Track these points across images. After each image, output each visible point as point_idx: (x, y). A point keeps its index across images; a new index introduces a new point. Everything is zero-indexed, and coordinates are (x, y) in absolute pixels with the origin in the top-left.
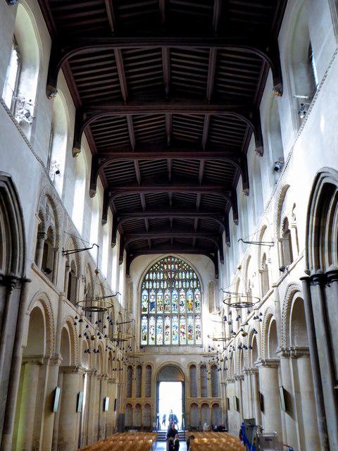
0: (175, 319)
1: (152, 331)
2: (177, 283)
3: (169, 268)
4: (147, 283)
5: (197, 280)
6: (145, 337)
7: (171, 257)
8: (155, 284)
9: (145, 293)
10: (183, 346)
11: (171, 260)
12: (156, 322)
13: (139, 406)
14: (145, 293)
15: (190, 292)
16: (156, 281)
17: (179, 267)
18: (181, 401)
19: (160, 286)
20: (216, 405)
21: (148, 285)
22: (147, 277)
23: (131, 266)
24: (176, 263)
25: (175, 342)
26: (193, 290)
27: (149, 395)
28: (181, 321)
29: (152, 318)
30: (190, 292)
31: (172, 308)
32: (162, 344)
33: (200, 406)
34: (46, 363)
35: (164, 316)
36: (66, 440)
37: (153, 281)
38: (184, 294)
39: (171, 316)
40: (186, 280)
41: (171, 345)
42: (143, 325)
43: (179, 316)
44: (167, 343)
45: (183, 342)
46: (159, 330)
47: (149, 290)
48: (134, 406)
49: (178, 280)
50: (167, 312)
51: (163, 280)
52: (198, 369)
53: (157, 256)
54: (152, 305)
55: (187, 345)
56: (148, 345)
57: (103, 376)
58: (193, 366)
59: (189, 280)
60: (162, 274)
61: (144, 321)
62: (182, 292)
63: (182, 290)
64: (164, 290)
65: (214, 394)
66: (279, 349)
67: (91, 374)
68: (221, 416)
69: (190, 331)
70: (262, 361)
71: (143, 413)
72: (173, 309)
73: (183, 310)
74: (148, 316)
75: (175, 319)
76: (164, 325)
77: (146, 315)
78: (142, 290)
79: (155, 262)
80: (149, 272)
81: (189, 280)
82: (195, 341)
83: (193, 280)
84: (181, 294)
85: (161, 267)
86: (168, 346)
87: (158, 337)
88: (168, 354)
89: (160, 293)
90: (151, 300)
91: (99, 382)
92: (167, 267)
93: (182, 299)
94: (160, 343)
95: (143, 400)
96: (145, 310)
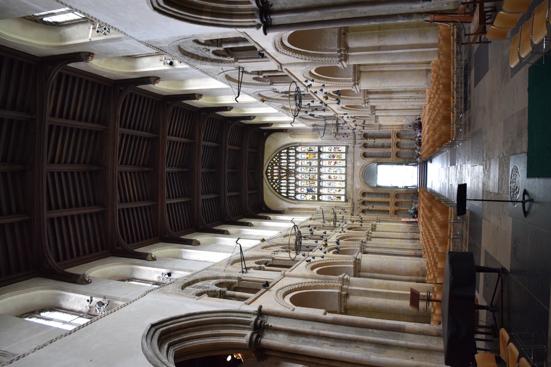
0: (322, 170)
1: (332, 192)
2: (290, 168)
3: (276, 174)
5: (288, 149)
6: (338, 197)
7: (267, 173)
8: (291, 188)
9: (298, 197)
10: (346, 163)
11: (269, 173)
12: (325, 187)
13: (396, 204)
14: (298, 197)
15: (299, 156)
16: (288, 186)
17: (276, 166)
19: (293, 183)
20: (398, 135)
22: (285, 195)
23: (274, 208)
24: (272, 168)
25: (343, 170)
26: (297, 153)
27: (387, 195)
28: (324, 165)
29: (322, 191)
30: (299, 156)
31: (313, 173)
32: (344, 182)
33: (398, 150)
35: (320, 180)
37: (288, 190)
38: (300, 161)
39: (320, 174)
40: (288, 159)
41: (346, 174)
42: (327, 200)
43: (320, 166)
44: (343, 177)
45: (343, 163)
46: (333, 184)
47: (296, 193)
49: (288, 166)
53: (265, 185)
54: (310, 191)
55: (346, 160)
56: (345, 195)
59: (288, 156)
60: (282, 181)
61: (323, 198)
62: (299, 163)
63: (297, 163)
64: (297, 180)
65: (389, 137)
69: (334, 157)
71: (403, 200)
72: (314, 172)
73: (315, 163)
74: (319, 194)
76: (328, 181)
78: (296, 199)
79: (271, 187)
80: (280, 193)
81: (288, 156)
82: (343, 153)
83: (288, 153)
84: (300, 164)
85: (276, 182)
86: (346, 177)
87: (338, 186)
88: (353, 177)
89: (299, 183)
90: (305, 191)
92: (276, 176)
93: (305, 163)
94: (343, 185)
96: (313, 198)
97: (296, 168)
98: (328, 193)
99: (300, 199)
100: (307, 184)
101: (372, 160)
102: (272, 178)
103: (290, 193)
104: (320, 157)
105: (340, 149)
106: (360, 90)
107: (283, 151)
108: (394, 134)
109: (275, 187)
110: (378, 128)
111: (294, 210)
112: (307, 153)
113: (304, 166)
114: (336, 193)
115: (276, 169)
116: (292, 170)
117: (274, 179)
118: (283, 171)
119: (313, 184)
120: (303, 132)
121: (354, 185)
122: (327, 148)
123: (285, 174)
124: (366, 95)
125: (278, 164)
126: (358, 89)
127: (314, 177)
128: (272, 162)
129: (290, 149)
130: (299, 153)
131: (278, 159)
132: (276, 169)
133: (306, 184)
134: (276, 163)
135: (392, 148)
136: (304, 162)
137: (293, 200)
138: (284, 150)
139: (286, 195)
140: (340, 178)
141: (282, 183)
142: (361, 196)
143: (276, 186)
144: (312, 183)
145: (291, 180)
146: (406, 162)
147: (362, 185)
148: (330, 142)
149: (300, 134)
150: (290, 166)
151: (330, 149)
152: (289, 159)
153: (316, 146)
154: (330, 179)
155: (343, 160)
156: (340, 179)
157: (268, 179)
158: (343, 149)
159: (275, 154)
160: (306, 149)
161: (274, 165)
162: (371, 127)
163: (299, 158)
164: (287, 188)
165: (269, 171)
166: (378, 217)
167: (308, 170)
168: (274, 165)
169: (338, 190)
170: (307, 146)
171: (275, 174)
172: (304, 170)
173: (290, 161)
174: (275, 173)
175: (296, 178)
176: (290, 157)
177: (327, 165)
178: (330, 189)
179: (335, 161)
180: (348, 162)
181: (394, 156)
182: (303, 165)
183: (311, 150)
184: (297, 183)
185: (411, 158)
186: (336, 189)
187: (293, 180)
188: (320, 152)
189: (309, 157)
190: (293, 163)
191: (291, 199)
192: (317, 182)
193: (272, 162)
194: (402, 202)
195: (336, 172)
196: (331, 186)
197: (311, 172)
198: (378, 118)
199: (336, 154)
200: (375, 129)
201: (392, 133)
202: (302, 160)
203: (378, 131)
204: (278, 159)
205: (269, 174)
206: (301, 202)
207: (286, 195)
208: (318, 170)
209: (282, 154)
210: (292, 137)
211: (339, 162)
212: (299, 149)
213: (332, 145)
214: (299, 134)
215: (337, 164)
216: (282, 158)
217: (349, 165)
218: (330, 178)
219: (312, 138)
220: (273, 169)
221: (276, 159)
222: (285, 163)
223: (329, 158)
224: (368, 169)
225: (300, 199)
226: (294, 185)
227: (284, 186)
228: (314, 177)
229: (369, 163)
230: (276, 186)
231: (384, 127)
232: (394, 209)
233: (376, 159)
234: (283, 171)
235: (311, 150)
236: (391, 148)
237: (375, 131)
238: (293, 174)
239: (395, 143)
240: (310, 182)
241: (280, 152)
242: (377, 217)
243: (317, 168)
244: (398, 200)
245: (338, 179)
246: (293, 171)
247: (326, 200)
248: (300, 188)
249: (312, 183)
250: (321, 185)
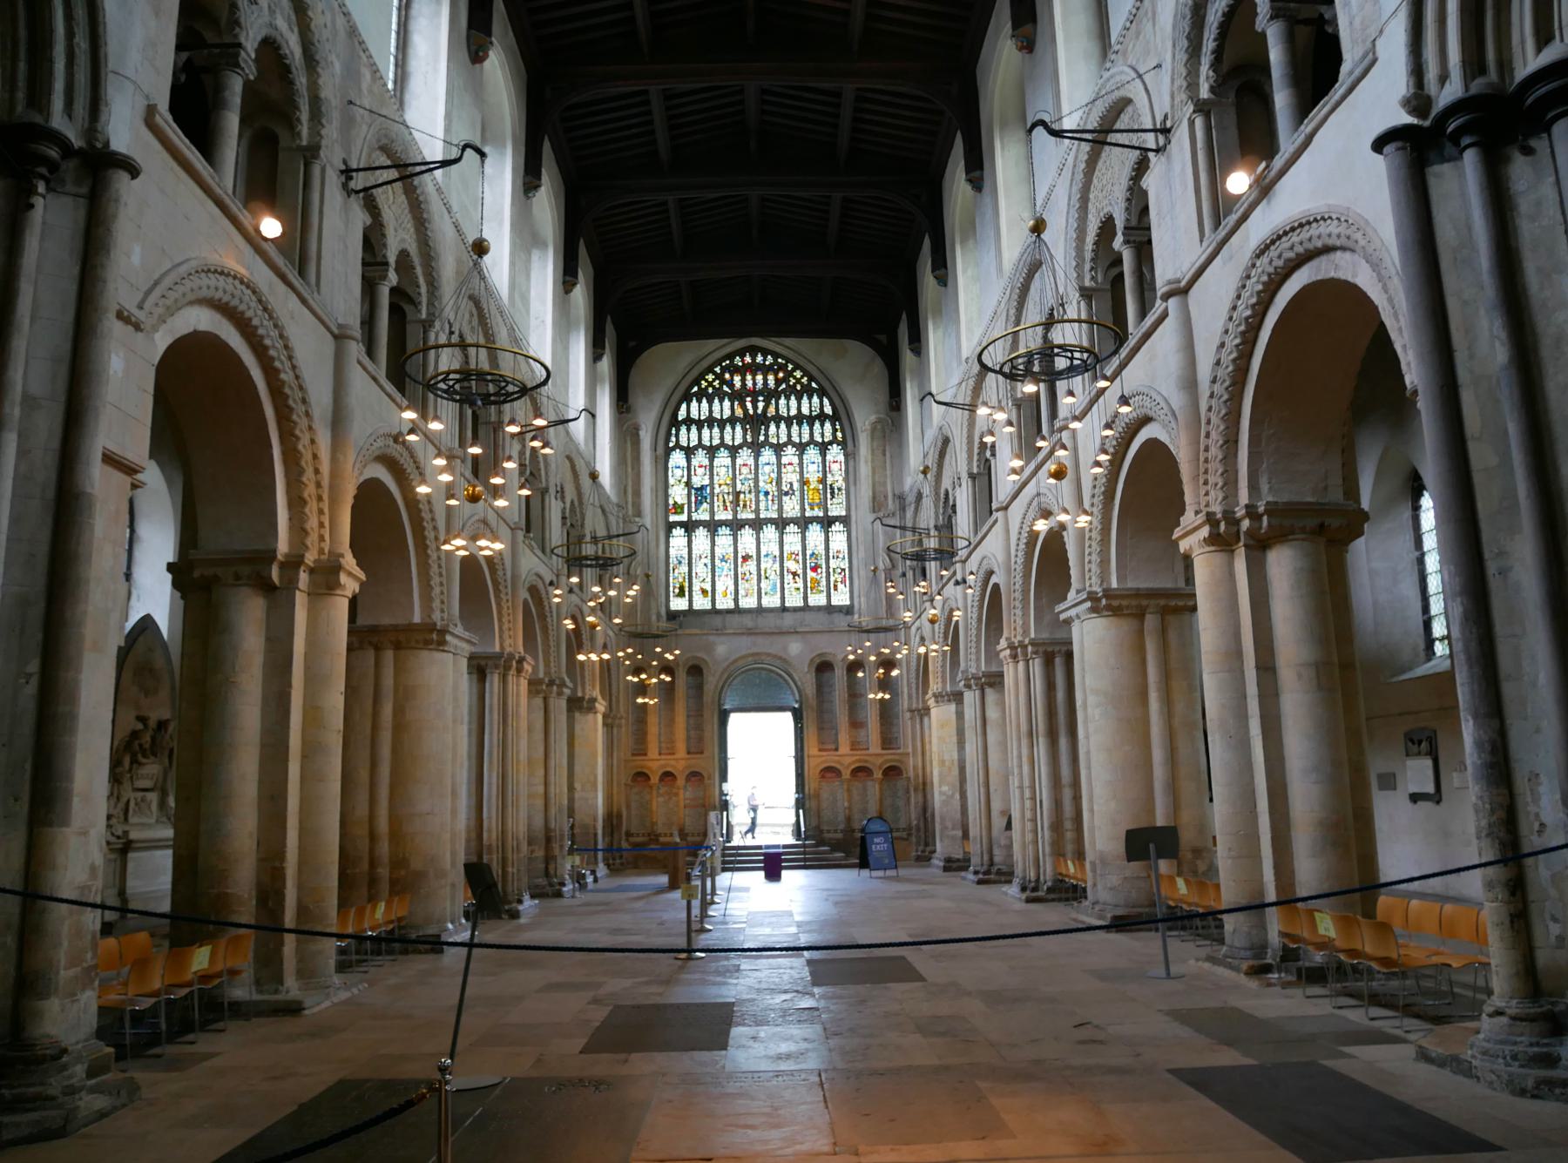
0: (770, 533)
1: (701, 570)
2: (773, 428)
3: (749, 384)
4: (683, 429)
5: (834, 418)
7: (753, 351)
8: (706, 432)
9: (677, 458)
10: (796, 610)
11: (754, 359)
13: (668, 776)
15: (812, 454)
16: (711, 421)
17: (778, 382)
18: (792, 762)
19: (722, 438)
20: (892, 772)
21: (688, 437)
22: (682, 414)
23: (635, 377)
25: (771, 601)
26: (823, 448)
30: (812, 454)
32: (731, 605)
33: (846, 774)
34: (291, 584)
35: (736, 526)
36: (416, 864)
37: (700, 424)
38: (795, 460)
39: (757, 525)
40: (800, 418)
41: (760, 610)
42: (672, 552)
43: (781, 524)
44: (748, 602)
45: (795, 600)
47: (689, 452)
48: (655, 779)
49: (778, 419)
50: (747, 515)
51: (733, 420)
52: (840, 674)
53: (712, 344)
54: (700, 495)
55: (806, 608)
56: (691, 612)
57: (551, 683)
58: (823, 667)
59: (811, 420)
60: (727, 403)
62: (790, 455)
63: (790, 450)
64: (734, 451)
65: (888, 741)
66: (1189, 518)
67: (507, 668)
68: (908, 800)
69: (814, 569)
70: (1092, 597)
71: (681, 796)
72: (762, 505)
73: (791, 507)
74: (689, 527)
75: (770, 533)
77: (681, 524)
78: (668, 452)
79: (705, 364)
80: (687, 398)
81: (811, 420)
83: (822, 417)
85: (723, 382)
86: (749, 611)
87: (720, 588)
88: (750, 632)
89: (723, 459)
90: (697, 481)
91: (539, 701)
92: (743, 380)
93: (790, 476)
94: (724, 603)
95: (679, 762)
96: (678, 508)
97: (772, 446)
98: (694, 556)
99: (670, 466)
100: (720, 485)
101: (810, 690)
102: (735, 370)
103: (689, 430)
104: (812, 523)
105: (840, 586)
106: (1068, 622)
107: (826, 401)
108: (897, 757)
109: (706, 381)
110: (914, 706)
111: (632, 444)
112: (823, 481)
113: (779, 473)
114: (694, 580)
115: (765, 380)
116: (767, 435)
117: (732, 376)
118: (761, 405)
119: (721, 504)
120: (892, 462)
121: (723, 638)
122: (843, 547)
123: (751, 412)
124: (1041, 649)
125: (784, 386)
126: (1072, 613)
127: (745, 506)
128: (790, 367)
129: (833, 425)
130: (823, 455)
131: (799, 387)
132: (765, 380)
133: (721, 482)
134: (785, 380)
135: (852, 755)
136: (795, 471)
137: (668, 440)
138: (832, 404)
139: (680, 418)
140: (747, 590)
141: (721, 401)
142: (690, 663)
143: (710, 384)
144: (724, 501)
145: (733, 432)
146: (807, 802)
147: (727, 663)
148: (861, 554)
149: (884, 455)
150: (778, 427)
151: (841, 556)
152: (800, 424)
153: (848, 509)
154: (740, 560)
155: (805, 598)
156: (742, 592)
157: (731, 356)
158: (841, 598)
159: (815, 373)
160: (836, 478)
161: (781, 375)
162: (917, 684)
163: (805, 457)
164: (705, 421)
165: (759, 359)
166: (623, 721)
167: (768, 487)
168: (781, 375)
169: (708, 587)
170: (846, 479)
171: (749, 377)
172: (767, 472)
173: (795, 428)
174: (754, 380)
175: (740, 446)
176: (808, 424)
177: (786, 548)
178: (708, 561)
179: (800, 572)
180: (799, 615)
181: (825, 762)
182: (784, 470)
183: (832, 494)
184: (723, 453)
185: (819, 817)
186: (709, 579)
187: (733, 439)
188: (827, 522)
189: (812, 487)
190: (789, 436)
191: (669, 434)
192: (730, 517)
193: (790, 367)
194: (677, 795)
195: (763, 577)
196: (717, 562)
197: (762, 497)
198: (949, 701)
199: (824, 575)
200: (910, 696)
201: (898, 751)
202: (801, 464)
203: (906, 706)
204: (799, 387)
205: (748, 359)
206: (661, 467)
207: (680, 418)
208: (771, 519)
209: (815, 399)
210: (873, 430)
211: (796, 586)
212: (835, 453)
213: (855, 562)
214: (884, 451)
215: (792, 581)
216: (805, 400)
217: (788, 620)
218: (746, 558)
219: (874, 493)
220: (765, 370)
221: (798, 381)
222: (788, 410)
223: (809, 552)
224: (781, 680)
225: (671, 464)
226: (716, 442)
227: (711, 411)
228: (745, 506)
229: (799, 683)
230: (710, 384)
231: (918, 726)
232: (649, 768)
233: (813, 702)
234: (761, 405)
235: (832, 494)
236: (852, 750)
237: (906, 696)
238: (752, 437)
239: (866, 761)
240: (728, 493)
241: (822, 393)
242: (621, 718)
243: (775, 515)
244: (681, 781)
245: (742, 586)
246: (762, 438)
247: (671, 549)
248: (706, 462)
249: (724, 501)
250: (720, 533)
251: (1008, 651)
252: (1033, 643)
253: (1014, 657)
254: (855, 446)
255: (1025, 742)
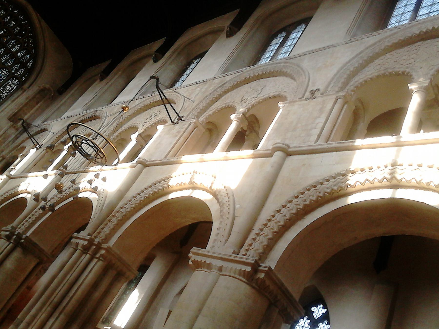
17: (20, 33)
24: (21, 26)
40: (13, 56)
59: (17, 61)
81: (17, 61)
83: (23, 65)
152: (11, 58)
241: (34, 57)
251: (86, 243)
252: (108, 250)
253: (85, 250)
254: (28, 88)
255: (48, 309)
